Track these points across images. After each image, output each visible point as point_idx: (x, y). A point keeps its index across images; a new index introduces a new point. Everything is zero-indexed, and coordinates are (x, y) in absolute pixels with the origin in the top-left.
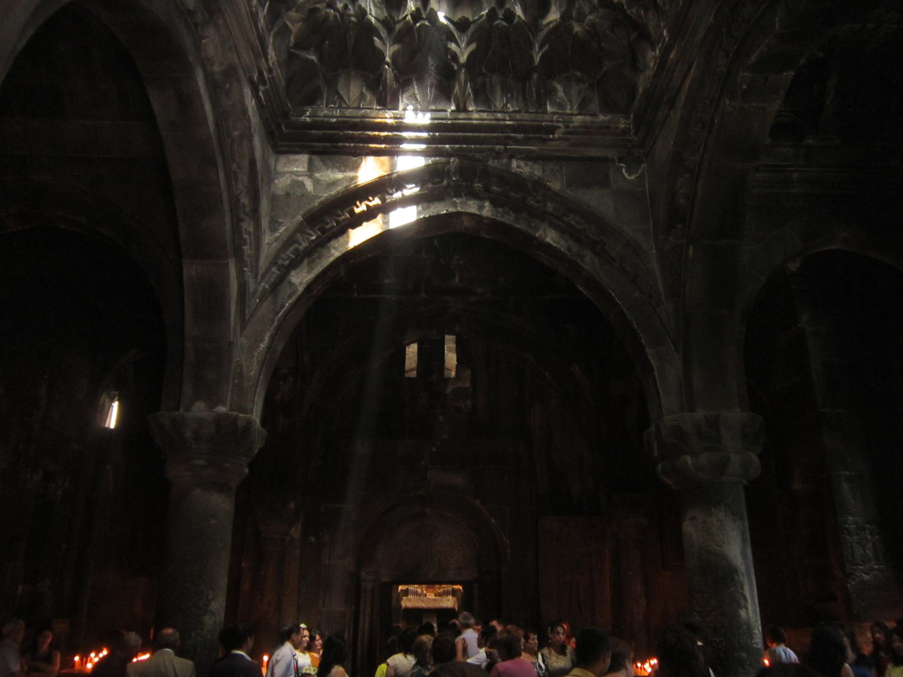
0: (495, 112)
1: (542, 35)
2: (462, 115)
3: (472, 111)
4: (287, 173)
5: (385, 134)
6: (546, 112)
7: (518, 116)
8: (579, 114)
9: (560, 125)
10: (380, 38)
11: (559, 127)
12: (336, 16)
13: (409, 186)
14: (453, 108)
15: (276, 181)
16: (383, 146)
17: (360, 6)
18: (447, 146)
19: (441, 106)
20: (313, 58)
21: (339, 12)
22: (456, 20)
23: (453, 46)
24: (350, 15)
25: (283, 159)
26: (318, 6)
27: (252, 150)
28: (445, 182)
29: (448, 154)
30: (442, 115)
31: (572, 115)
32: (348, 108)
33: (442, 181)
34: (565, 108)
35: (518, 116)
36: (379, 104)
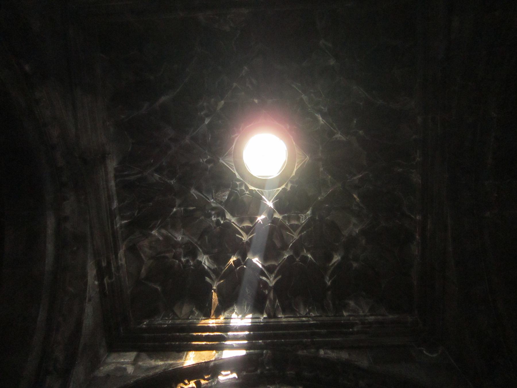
0: (300, 317)
1: (330, 272)
2: (272, 320)
3: (282, 317)
4: (113, 363)
5: (207, 334)
6: (343, 316)
7: (320, 319)
8: (371, 315)
9: (357, 321)
10: (210, 278)
11: (357, 323)
12: (179, 265)
13: (223, 373)
14: (265, 316)
15: (102, 368)
16: (204, 343)
17: (198, 260)
18: (260, 341)
19: (256, 315)
20: (159, 288)
21: (182, 263)
22: (266, 265)
23: (264, 278)
24: (191, 266)
25: (114, 355)
26: (167, 255)
27: (82, 310)
28: (259, 371)
29: (261, 347)
30: (257, 320)
31: (365, 316)
32: (179, 319)
33: (256, 370)
34: (358, 311)
35: (320, 319)
36: (204, 316)
